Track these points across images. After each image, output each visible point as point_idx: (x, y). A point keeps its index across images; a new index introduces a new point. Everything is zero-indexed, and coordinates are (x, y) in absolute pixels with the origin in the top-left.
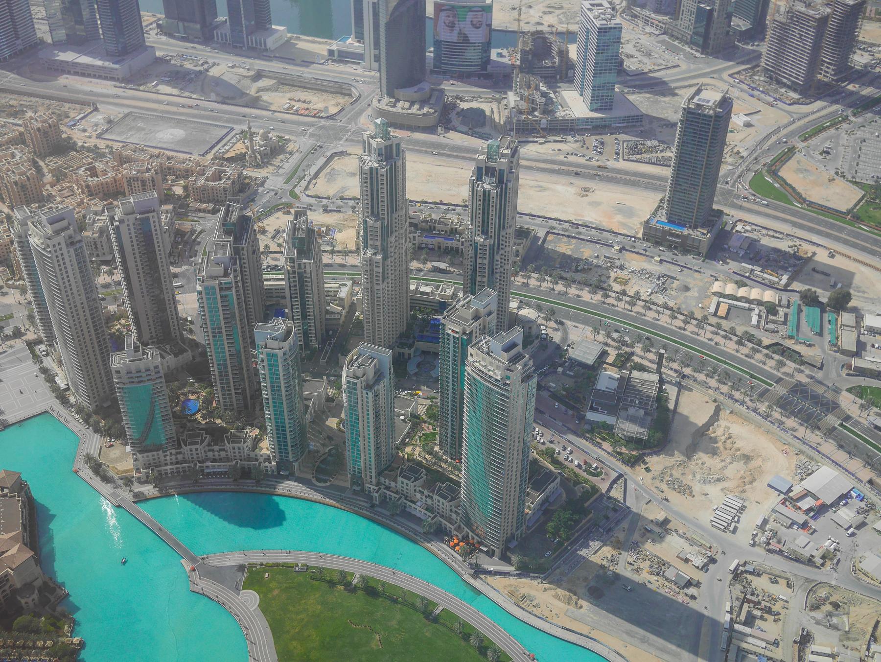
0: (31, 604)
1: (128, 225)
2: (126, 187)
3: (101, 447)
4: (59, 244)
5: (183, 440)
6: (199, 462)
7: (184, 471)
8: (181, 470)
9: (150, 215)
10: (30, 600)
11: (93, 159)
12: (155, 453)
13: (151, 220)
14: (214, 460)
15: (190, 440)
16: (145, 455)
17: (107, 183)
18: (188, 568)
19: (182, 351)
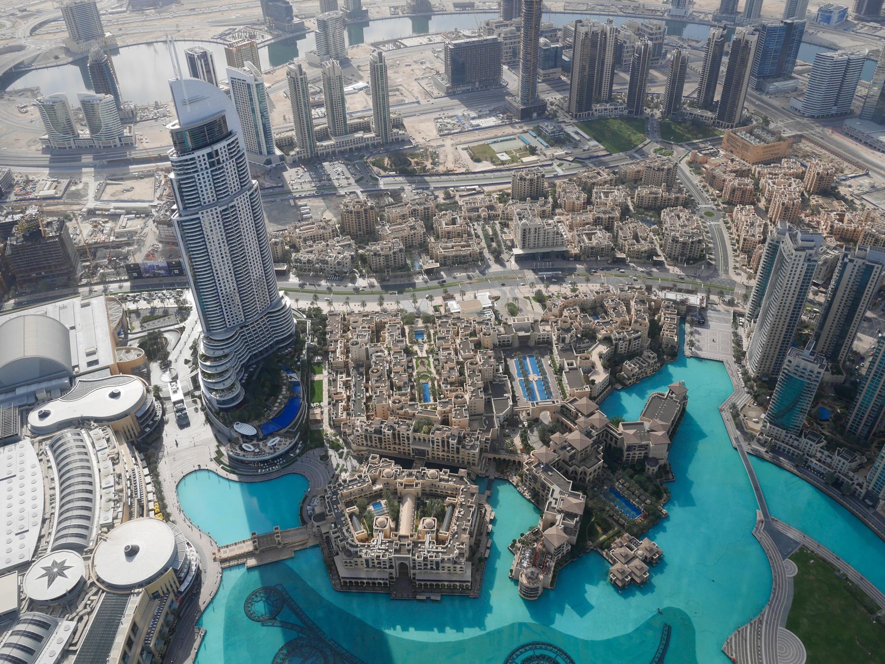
0: (651, 472)
1: (855, 266)
2: (861, 237)
3: (745, 405)
4: (800, 256)
5: (805, 433)
6: (808, 455)
7: (793, 454)
8: (791, 452)
9: (876, 266)
10: (651, 469)
11: (846, 209)
12: (780, 430)
13: (875, 269)
14: (819, 461)
15: (809, 436)
16: (773, 427)
17: (847, 230)
18: (758, 518)
19: (839, 372)
